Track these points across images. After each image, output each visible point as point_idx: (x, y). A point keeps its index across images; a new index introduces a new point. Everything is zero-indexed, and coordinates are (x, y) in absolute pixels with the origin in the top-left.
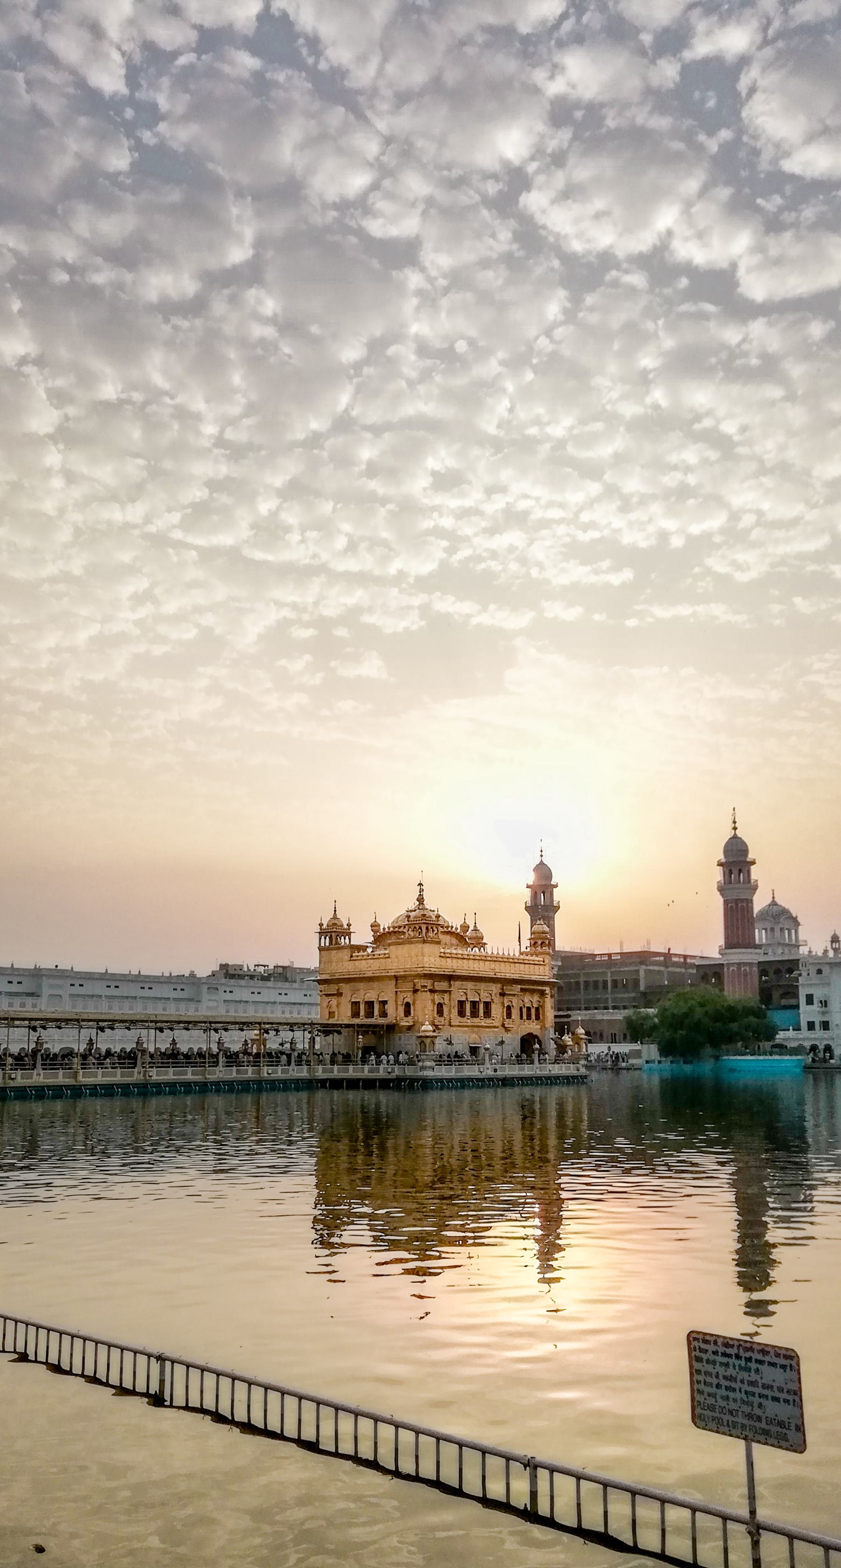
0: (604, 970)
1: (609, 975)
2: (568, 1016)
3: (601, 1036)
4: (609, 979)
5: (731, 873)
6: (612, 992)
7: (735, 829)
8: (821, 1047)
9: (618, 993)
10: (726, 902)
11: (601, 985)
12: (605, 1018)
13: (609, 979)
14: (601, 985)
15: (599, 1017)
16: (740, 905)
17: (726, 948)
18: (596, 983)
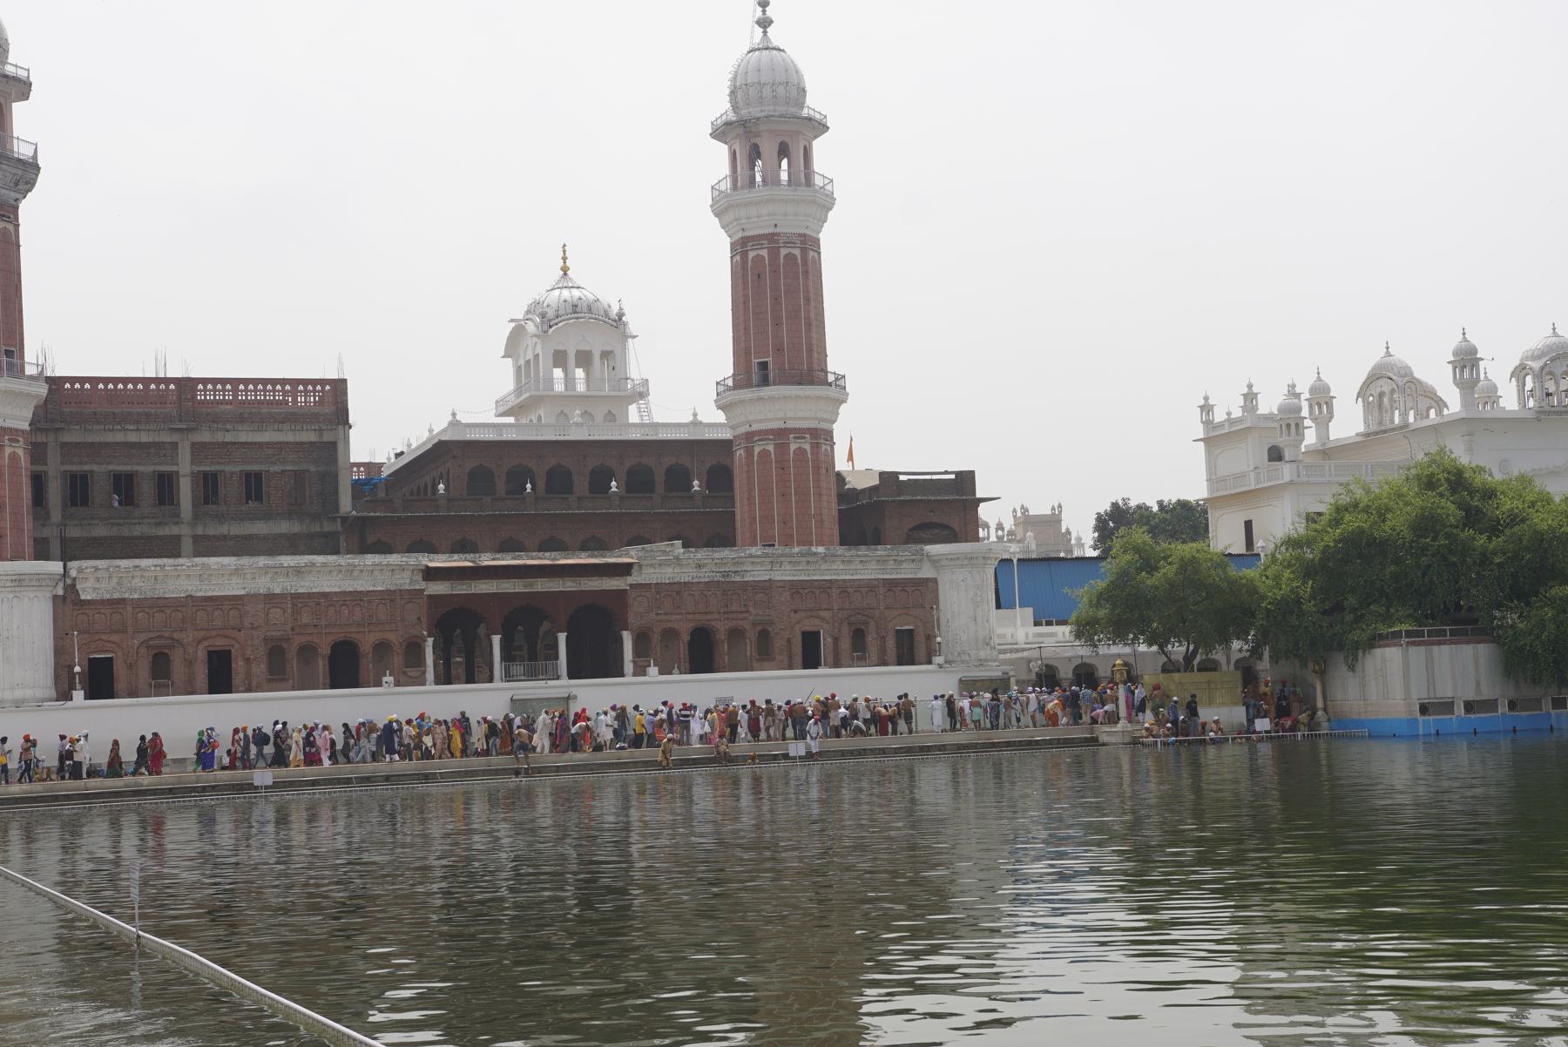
0: (165, 437)
1: (185, 454)
2: (625, 570)
3: (764, 639)
4: (184, 467)
5: (755, 153)
6: (197, 517)
7: (765, 23)
8: (1066, 673)
9: (220, 518)
10: (741, 248)
11: (146, 491)
12: (784, 574)
13: (184, 467)
14: (146, 491)
15: (759, 574)
16: (751, 255)
17: (737, 386)
18: (124, 486)
